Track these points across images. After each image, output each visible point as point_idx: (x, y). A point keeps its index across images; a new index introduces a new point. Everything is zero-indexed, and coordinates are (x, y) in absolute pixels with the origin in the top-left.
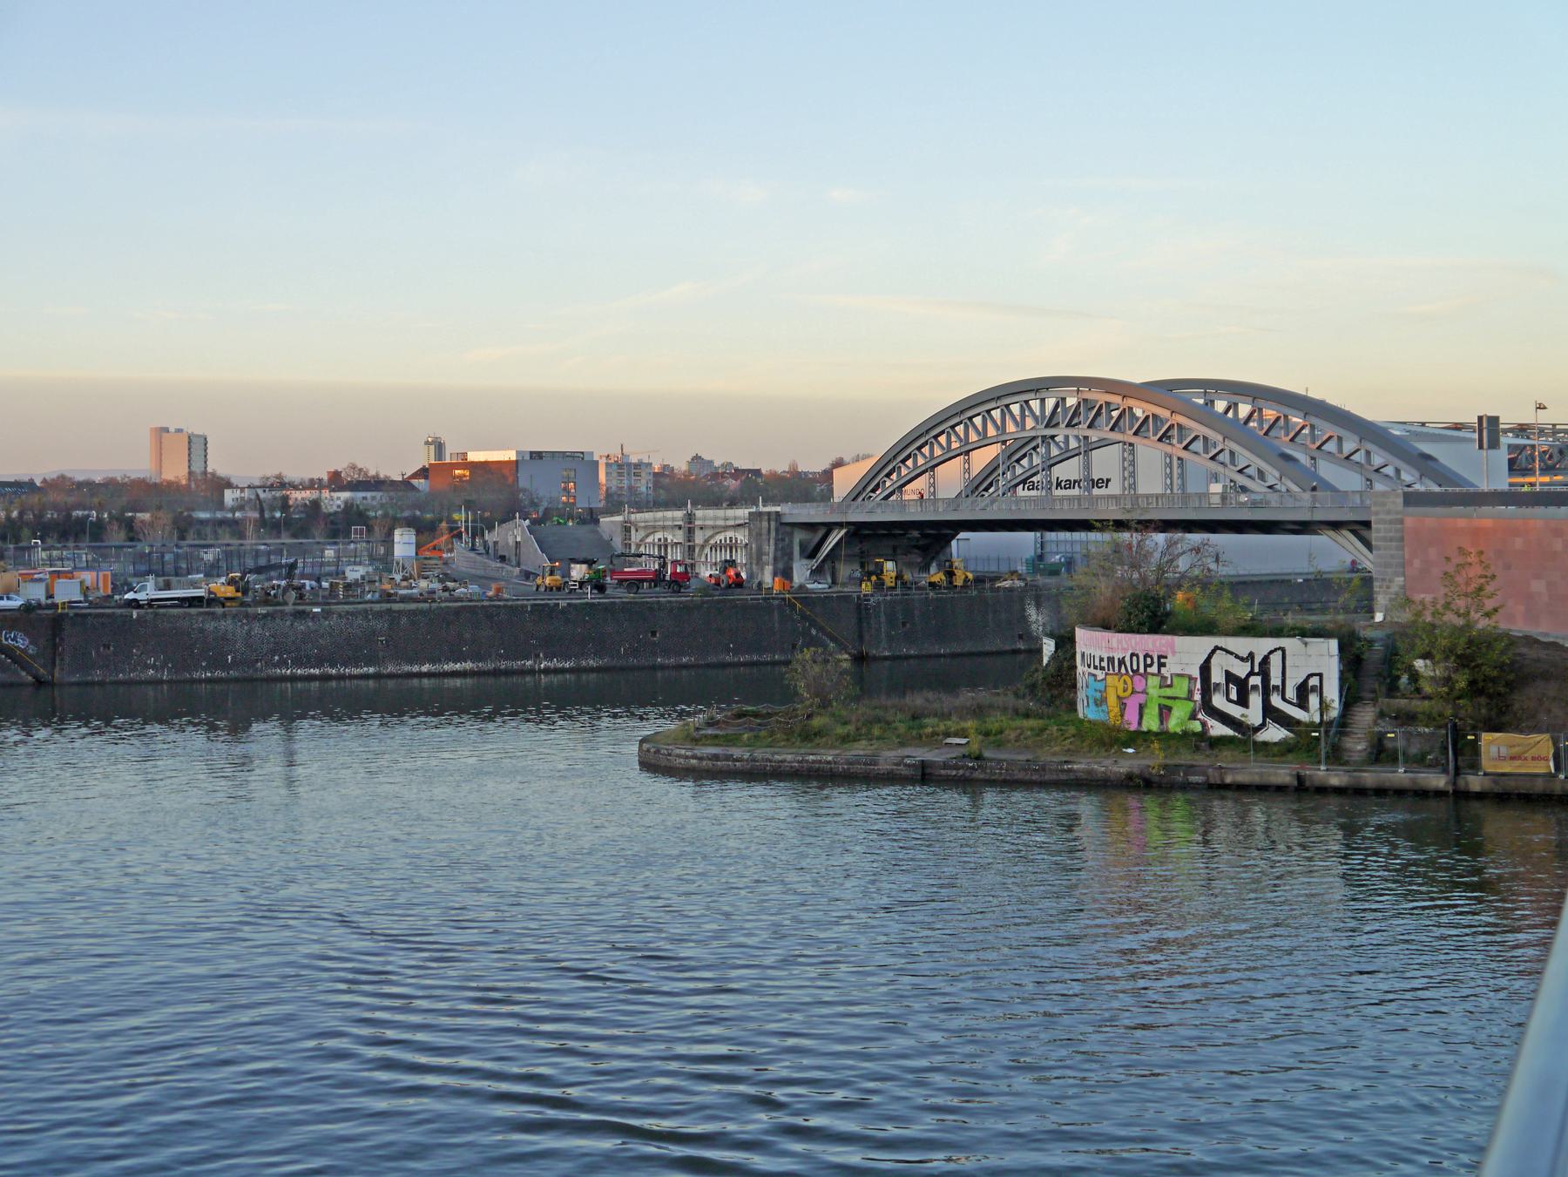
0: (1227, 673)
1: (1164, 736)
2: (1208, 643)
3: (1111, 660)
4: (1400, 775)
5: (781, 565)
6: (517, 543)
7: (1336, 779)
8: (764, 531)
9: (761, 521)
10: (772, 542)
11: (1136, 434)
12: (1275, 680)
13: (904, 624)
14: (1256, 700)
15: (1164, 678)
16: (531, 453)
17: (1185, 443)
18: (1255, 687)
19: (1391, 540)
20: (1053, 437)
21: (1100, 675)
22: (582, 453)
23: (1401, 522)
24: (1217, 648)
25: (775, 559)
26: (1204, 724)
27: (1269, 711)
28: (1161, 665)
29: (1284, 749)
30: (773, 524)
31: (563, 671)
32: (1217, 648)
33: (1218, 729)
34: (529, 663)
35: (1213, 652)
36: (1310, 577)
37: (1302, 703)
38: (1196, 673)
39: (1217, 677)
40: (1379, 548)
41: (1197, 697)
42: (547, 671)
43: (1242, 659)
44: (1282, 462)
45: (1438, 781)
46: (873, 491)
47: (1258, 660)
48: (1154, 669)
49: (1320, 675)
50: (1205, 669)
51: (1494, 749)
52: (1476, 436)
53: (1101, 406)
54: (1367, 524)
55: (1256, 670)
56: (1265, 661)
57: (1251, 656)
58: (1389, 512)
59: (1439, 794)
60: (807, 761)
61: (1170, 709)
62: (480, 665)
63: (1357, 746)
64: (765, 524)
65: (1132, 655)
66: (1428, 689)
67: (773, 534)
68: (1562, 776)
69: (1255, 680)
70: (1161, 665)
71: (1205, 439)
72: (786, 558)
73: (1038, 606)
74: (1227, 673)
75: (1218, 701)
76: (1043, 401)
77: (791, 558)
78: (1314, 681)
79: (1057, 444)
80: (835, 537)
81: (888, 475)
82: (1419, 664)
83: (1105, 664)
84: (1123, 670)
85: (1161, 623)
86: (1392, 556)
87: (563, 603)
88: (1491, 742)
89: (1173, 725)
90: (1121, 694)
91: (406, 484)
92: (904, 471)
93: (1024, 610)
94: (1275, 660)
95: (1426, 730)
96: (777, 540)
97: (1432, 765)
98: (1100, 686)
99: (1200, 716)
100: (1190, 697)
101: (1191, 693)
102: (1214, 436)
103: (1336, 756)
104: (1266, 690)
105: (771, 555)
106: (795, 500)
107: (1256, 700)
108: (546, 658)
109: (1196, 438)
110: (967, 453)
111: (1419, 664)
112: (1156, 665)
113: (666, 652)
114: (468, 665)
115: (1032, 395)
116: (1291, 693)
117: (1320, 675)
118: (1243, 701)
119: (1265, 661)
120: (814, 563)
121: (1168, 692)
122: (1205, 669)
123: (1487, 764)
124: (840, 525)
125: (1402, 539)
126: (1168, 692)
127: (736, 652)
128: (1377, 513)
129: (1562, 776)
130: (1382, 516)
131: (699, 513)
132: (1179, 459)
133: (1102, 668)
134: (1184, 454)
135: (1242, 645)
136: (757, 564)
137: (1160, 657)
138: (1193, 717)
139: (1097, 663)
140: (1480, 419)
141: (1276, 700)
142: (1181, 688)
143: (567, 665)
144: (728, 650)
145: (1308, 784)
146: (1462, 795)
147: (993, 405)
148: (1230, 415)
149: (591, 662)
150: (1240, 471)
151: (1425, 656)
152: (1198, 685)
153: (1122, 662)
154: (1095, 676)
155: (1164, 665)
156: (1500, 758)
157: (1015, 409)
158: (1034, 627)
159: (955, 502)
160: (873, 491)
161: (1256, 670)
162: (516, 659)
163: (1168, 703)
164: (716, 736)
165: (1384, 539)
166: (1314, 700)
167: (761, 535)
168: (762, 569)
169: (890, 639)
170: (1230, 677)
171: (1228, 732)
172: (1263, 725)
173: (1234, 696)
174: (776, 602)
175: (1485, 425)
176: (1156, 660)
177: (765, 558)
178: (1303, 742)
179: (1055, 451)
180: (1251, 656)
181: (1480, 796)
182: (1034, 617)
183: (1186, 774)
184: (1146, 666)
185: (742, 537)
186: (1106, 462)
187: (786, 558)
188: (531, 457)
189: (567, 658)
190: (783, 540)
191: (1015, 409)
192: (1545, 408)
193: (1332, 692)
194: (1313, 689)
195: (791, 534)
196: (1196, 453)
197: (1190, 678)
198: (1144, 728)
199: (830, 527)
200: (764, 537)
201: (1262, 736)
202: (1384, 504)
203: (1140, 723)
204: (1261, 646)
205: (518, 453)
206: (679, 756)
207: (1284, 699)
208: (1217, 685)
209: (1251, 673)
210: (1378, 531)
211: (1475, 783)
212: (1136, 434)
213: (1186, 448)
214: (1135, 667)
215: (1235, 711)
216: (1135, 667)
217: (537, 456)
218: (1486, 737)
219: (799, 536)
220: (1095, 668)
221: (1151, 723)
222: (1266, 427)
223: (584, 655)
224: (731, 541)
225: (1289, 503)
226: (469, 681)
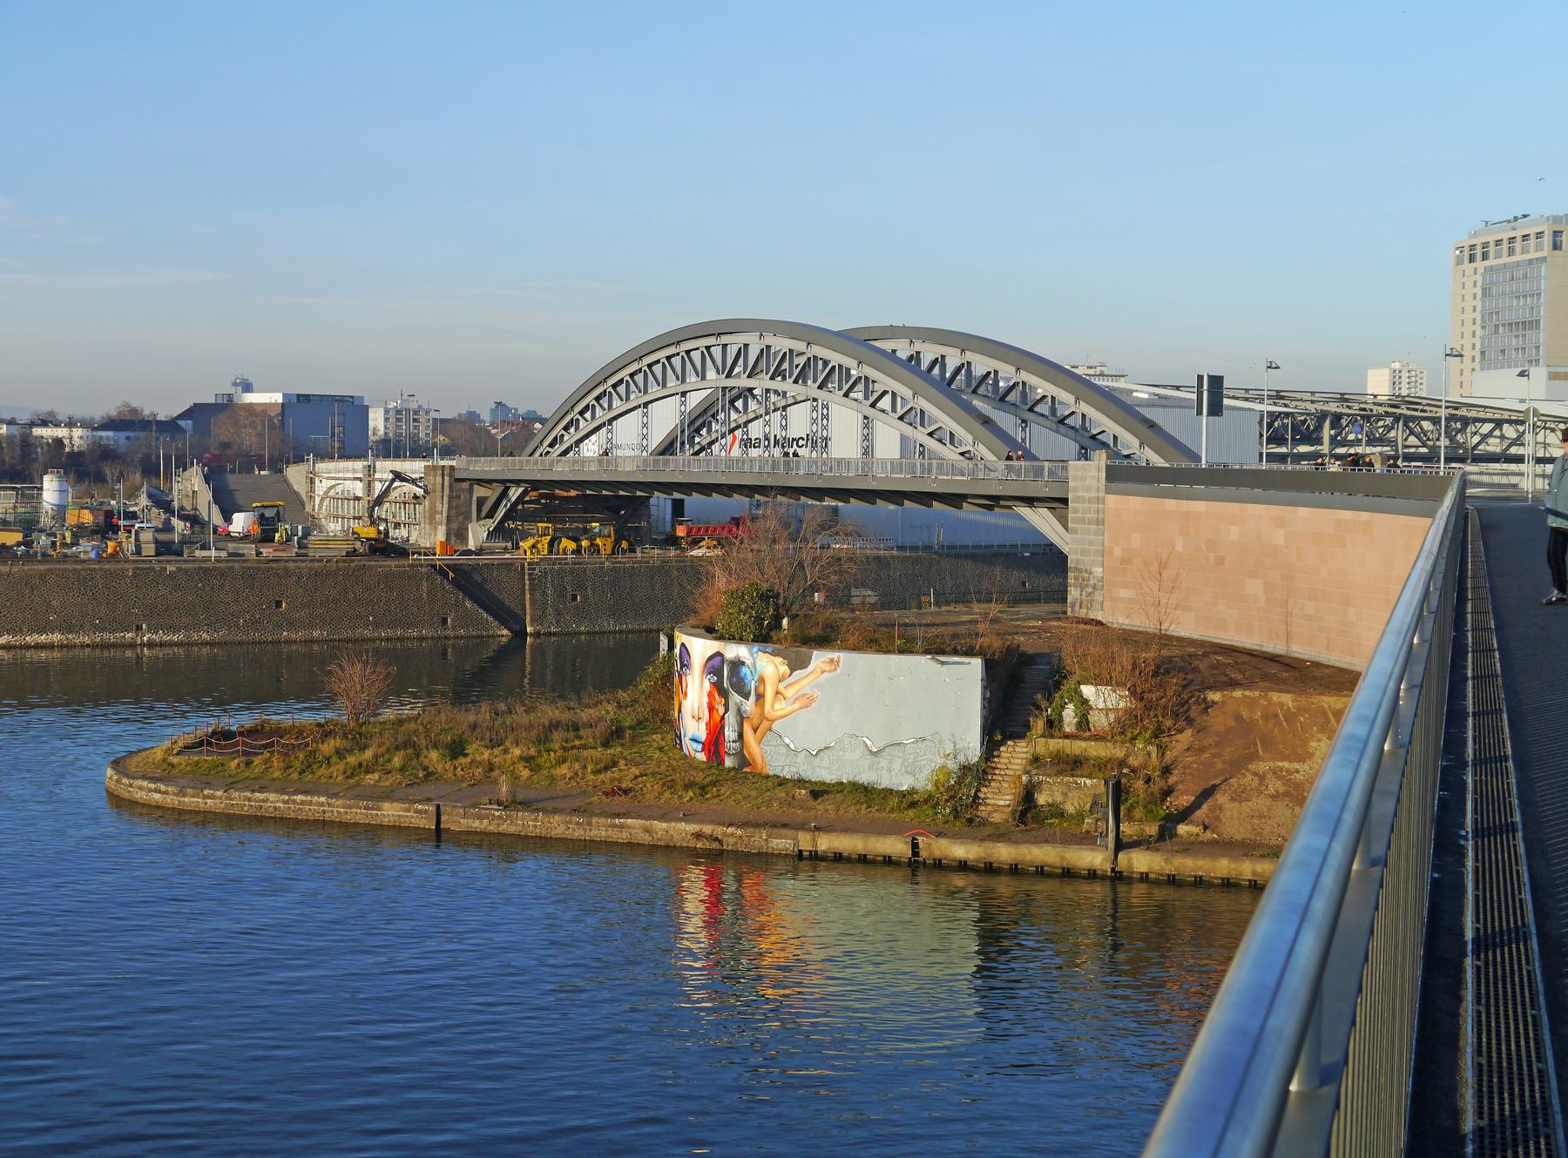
5: (455, 526)
6: (194, 492)
9: (435, 476)
10: (446, 499)
11: (820, 387)
16: (298, 395)
17: (872, 399)
20: (750, 390)
22: (352, 397)
25: (449, 519)
31: (171, 644)
34: (129, 635)
36: (1036, 550)
40: (1075, 531)
42: (151, 645)
46: (551, 445)
52: (1194, 396)
58: (1088, 489)
59: (1092, 875)
60: (294, 802)
62: (70, 636)
63: (1000, 800)
64: (439, 479)
66: (1099, 721)
67: (447, 492)
71: (894, 395)
72: (461, 518)
76: (725, 346)
77: (468, 518)
79: (754, 397)
80: (515, 493)
81: (566, 428)
82: (1088, 691)
86: (1091, 543)
87: (171, 568)
91: (171, 426)
95: (1088, 782)
96: (450, 497)
102: (904, 391)
105: (445, 515)
106: (473, 453)
108: (149, 631)
109: (885, 393)
110: (646, 405)
111: (1088, 691)
113: (291, 625)
114: (56, 637)
120: (491, 524)
124: (518, 482)
125: (1100, 522)
127: (377, 625)
128: (1075, 490)
130: (1080, 494)
131: (379, 464)
134: (871, 412)
136: (430, 523)
140: (1200, 378)
148: (936, 371)
149: (204, 635)
150: (931, 434)
157: (696, 356)
162: (113, 631)
165: (1082, 521)
168: (436, 529)
169: (558, 613)
174: (424, 570)
177: (438, 517)
179: (752, 405)
186: (799, 421)
187: (461, 518)
188: (298, 400)
189: (174, 629)
190: (458, 497)
191: (696, 356)
192: (1278, 368)
195: (471, 491)
196: (883, 411)
199: (506, 484)
202: (1083, 479)
205: (285, 396)
206: (141, 788)
210: (1076, 511)
212: (820, 387)
213: (873, 405)
217: (304, 399)
222: (974, 384)
223: (195, 626)
226: (57, 654)
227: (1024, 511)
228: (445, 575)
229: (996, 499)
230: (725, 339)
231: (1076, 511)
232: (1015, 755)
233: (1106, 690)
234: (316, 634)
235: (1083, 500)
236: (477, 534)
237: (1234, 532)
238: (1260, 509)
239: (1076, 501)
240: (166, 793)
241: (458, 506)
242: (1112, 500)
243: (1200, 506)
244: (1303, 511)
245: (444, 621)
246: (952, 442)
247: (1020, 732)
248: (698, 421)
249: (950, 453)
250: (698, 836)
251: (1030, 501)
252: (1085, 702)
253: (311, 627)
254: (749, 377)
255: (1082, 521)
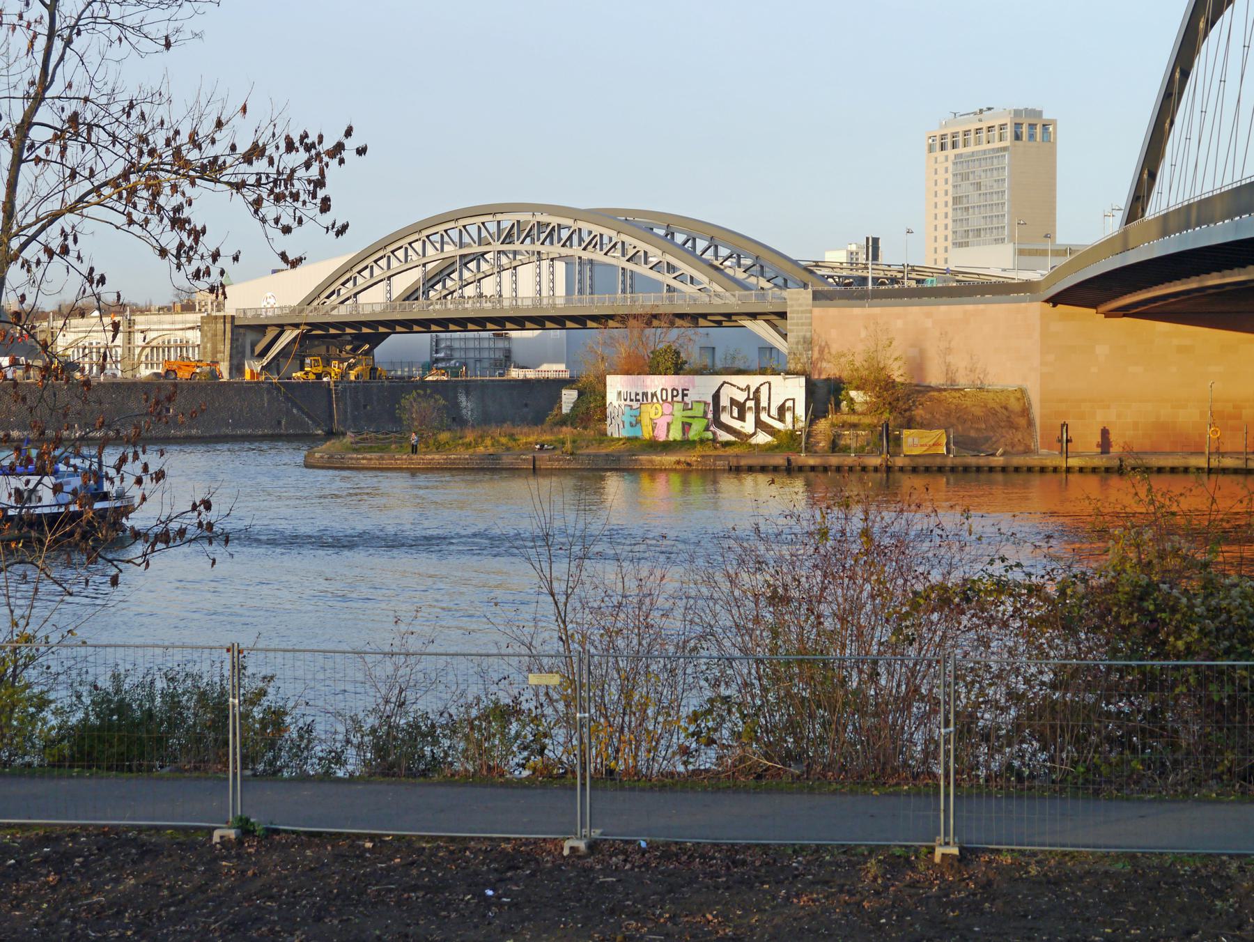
0: (731, 399)
1: (685, 444)
2: (719, 379)
3: (645, 394)
4: (850, 459)
5: (235, 362)
7: (812, 461)
8: (220, 332)
9: (216, 323)
10: (228, 342)
12: (764, 403)
13: (365, 407)
14: (750, 417)
15: (686, 404)
18: (750, 408)
19: (802, 324)
21: (636, 405)
23: (811, 312)
24: (725, 383)
25: (231, 356)
26: (714, 434)
27: (759, 424)
28: (684, 395)
29: (768, 448)
30: (228, 326)
32: (725, 383)
33: (724, 436)
35: (722, 385)
37: (781, 418)
38: (710, 400)
39: (724, 401)
41: (710, 416)
43: (742, 390)
44: (712, 271)
45: (875, 461)
46: (328, 297)
47: (752, 390)
48: (679, 398)
49: (794, 400)
50: (716, 397)
51: (910, 440)
53: (554, 227)
54: (783, 315)
55: (751, 397)
56: (758, 390)
57: (748, 387)
58: (800, 305)
61: (690, 425)
62: (25, 433)
64: (220, 326)
65: (662, 390)
66: (858, 408)
67: (228, 335)
68: (951, 456)
69: (751, 404)
70: (684, 395)
73: (467, 394)
74: (731, 399)
75: (725, 418)
77: (244, 357)
78: (789, 404)
81: (343, 284)
82: (853, 394)
83: (640, 397)
84: (655, 400)
85: (681, 368)
88: (909, 436)
89: (693, 435)
90: (653, 416)
92: (360, 280)
93: (456, 397)
94: (764, 390)
97: (871, 453)
98: (635, 413)
99: (712, 428)
100: (705, 416)
101: (705, 413)
103: (809, 449)
104: (758, 409)
107: (750, 417)
111: (853, 394)
112: (680, 395)
115: (490, 218)
116: (774, 412)
117: (794, 400)
118: (742, 417)
119: (758, 390)
121: (689, 413)
122: (716, 397)
123: (906, 449)
126: (689, 413)
128: (792, 306)
129: (951, 456)
130: (795, 308)
132: (623, 269)
133: (637, 400)
134: (630, 266)
135: (741, 380)
137: (683, 390)
138: (707, 429)
139: (633, 397)
140: (868, 239)
141: (764, 417)
142: (698, 411)
143: (98, 435)
144: (228, 425)
145: (794, 464)
146: (889, 469)
147: (452, 225)
151: (857, 388)
152: (711, 408)
153: (654, 395)
154: (631, 406)
155: (686, 395)
156: (914, 445)
158: (464, 411)
159: (383, 312)
160: (328, 297)
161: (751, 397)
163: (689, 420)
164: (371, 447)
165: (797, 325)
166: (789, 416)
167: (216, 335)
170: (733, 402)
171: (731, 438)
172: (754, 434)
173: (735, 414)
174: (265, 386)
175: (870, 243)
176: (680, 392)
178: (790, 441)
180: (748, 387)
181: (902, 469)
182: (464, 404)
183: (715, 460)
184: (673, 396)
185: (194, 337)
190: (237, 340)
193: (800, 410)
194: (789, 409)
197: (705, 403)
198: (671, 438)
200: (220, 337)
201: (754, 441)
203: (667, 436)
204: (754, 381)
206: (352, 459)
207: (769, 415)
208: (724, 408)
209: (748, 399)
211: (899, 461)
214: (664, 398)
215: (736, 424)
216: (664, 398)
218: (906, 432)
219: (250, 337)
220: (631, 400)
221: (676, 434)
224: (169, 342)
225: (717, 301)
227: (748, 323)
228: (279, 389)
229: (728, 316)
230: (499, 217)
231: (792, 318)
232: (822, 425)
233: (861, 393)
234: (194, 432)
235: (798, 312)
236: (252, 367)
237: (899, 323)
238: (915, 309)
239: (792, 312)
240: (371, 459)
241: (237, 346)
242: (817, 311)
243: (877, 310)
244: (943, 308)
245: (279, 423)
246: (692, 282)
247: (824, 414)
248: (431, 281)
249: (688, 289)
250: (678, 462)
251: (753, 316)
252: (852, 399)
253: (191, 427)
254: (502, 243)
255: (797, 325)
